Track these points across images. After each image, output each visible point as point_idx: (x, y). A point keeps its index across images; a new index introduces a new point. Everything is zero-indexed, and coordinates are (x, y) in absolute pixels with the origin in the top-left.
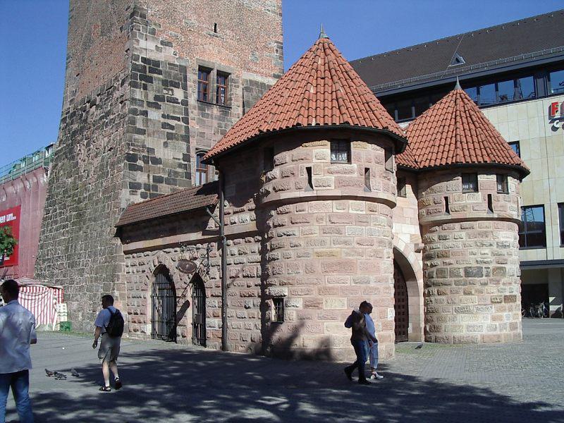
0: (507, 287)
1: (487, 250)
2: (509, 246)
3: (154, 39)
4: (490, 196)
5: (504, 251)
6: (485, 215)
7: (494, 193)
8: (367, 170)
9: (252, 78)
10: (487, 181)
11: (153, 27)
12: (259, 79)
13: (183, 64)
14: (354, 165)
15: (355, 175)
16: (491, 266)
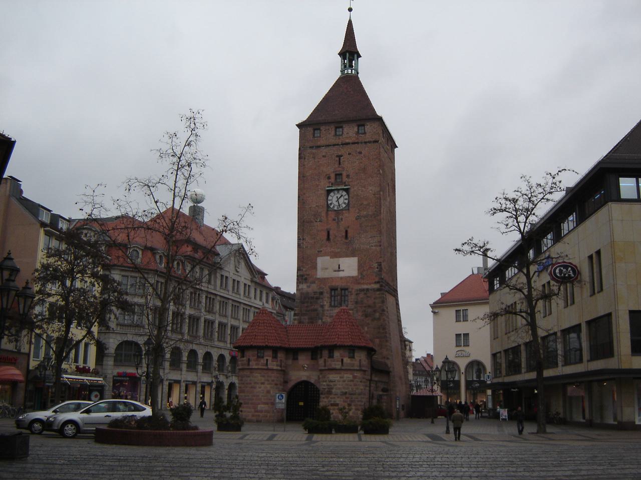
0: (333, 400)
1: (324, 384)
2: (335, 381)
3: (306, 282)
4: (325, 359)
5: (332, 384)
6: (323, 368)
7: (326, 358)
8: (249, 359)
9: (360, 288)
10: (325, 353)
11: (306, 276)
12: (365, 287)
13: (322, 291)
14: (245, 358)
15: (245, 361)
16: (326, 390)
